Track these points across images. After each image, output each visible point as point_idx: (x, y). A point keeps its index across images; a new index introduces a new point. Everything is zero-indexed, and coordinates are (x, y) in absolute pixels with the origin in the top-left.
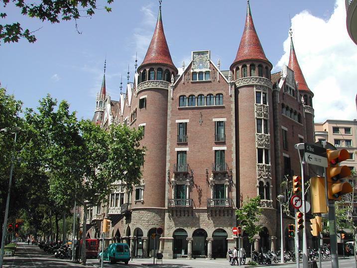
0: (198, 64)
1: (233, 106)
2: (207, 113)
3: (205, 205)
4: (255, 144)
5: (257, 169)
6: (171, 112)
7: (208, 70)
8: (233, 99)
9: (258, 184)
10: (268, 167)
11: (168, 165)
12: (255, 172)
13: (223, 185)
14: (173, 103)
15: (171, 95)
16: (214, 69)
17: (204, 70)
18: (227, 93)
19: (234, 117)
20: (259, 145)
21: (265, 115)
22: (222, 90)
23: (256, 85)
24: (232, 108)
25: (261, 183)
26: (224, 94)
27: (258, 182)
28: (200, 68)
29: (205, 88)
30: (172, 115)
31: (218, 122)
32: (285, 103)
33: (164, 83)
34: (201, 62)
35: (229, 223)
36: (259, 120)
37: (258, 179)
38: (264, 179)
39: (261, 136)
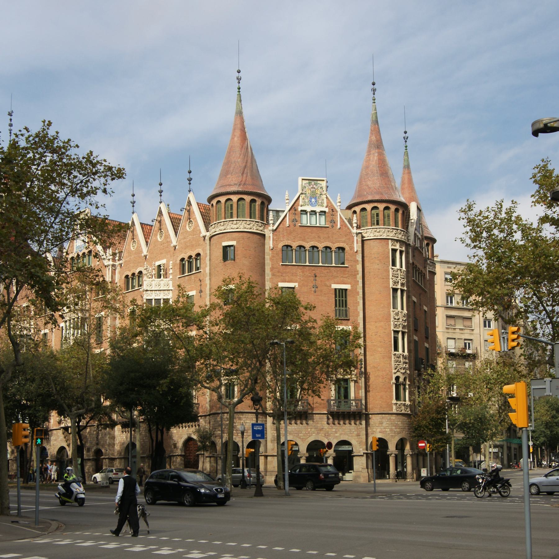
0: (309, 199)
1: (359, 267)
2: (322, 275)
3: (323, 408)
4: (390, 325)
5: (393, 359)
6: (272, 269)
7: (324, 209)
8: (359, 258)
9: (394, 381)
10: (405, 358)
12: (390, 364)
13: (346, 381)
14: (273, 257)
15: (270, 243)
16: (333, 210)
17: (318, 209)
18: (352, 248)
19: (361, 284)
20: (396, 326)
21: (402, 285)
22: (344, 242)
23: (392, 239)
24: (358, 271)
25: (397, 378)
26: (347, 248)
27: (394, 376)
28: (312, 205)
29: (319, 237)
30: (273, 275)
31: (340, 290)
32: (415, 262)
33: (260, 224)
34: (314, 195)
35: (356, 433)
36: (395, 290)
37: (395, 373)
38: (401, 373)
39: (397, 314)
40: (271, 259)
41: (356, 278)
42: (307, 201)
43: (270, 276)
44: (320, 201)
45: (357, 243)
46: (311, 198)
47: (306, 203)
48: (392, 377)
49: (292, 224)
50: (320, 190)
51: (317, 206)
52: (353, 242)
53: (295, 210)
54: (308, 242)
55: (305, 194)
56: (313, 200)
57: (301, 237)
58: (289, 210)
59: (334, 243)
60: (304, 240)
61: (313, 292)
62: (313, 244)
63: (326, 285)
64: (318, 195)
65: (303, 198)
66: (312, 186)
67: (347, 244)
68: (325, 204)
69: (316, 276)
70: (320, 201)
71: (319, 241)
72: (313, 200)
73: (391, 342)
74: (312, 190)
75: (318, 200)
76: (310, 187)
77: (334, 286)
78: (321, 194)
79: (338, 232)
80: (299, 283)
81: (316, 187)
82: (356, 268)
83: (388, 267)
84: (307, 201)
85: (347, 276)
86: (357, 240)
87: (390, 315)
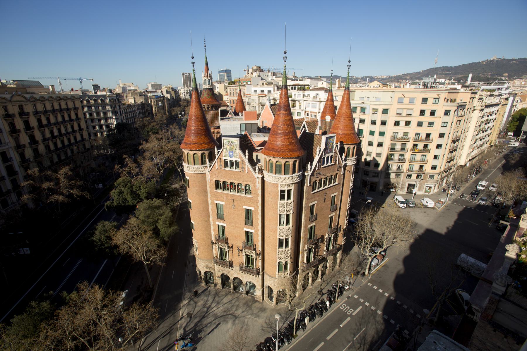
11: (213, 233)
12: (276, 255)
14: (211, 186)
15: (208, 179)
18: (255, 186)
24: (259, 200)
27: (278, 262)
40: (209, 187)
41: (257, 204)
42: (227, 154)
43: (210, 196)
44: (235, 154)
45: (258, 183)
46: (230, 152)
47: (227, 155)
48: (276, 262)
49: (219, 168)
50: (235, 147)
51: (233, 157)
52: (256, 182)
53: (221, 159)
54: (229, 180)
55: (226, 149)
56: (231, 153)
57: (225, 176)
58: (217, 159)
59: (244, 182)
60: (227, 178)
61: (233, 209)
62: (231, 181)
63: (239, 206)
64: (234, 150)
65: (224, 151)
66: (230, 144)
67: (252, 183)
68: (238, 157)
69: (234, 200)
70: (235, 154)
71: (235, 180)
72: (231, 153)
73: (277, 244)
74: (230, 146)
75: (234, 153)
76: (229, 145)
77: (245, 207)
78: (236, 150)
79: (246, 175)
80: (225, 202)
81: (233, 145)
82: (258, 199)
83: (277, 201)
84: (227, 154)
85: (252, 202)
86: (258, 181)
87: (277, 229)
